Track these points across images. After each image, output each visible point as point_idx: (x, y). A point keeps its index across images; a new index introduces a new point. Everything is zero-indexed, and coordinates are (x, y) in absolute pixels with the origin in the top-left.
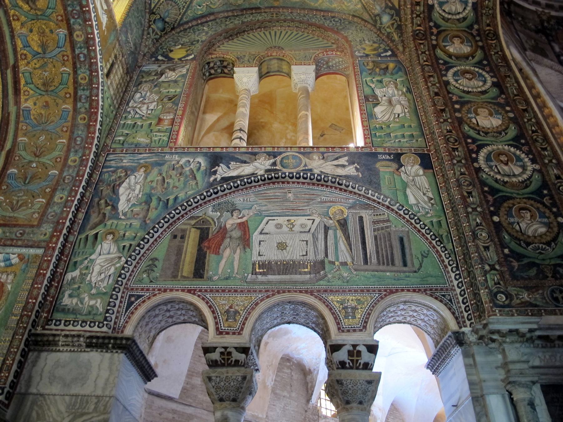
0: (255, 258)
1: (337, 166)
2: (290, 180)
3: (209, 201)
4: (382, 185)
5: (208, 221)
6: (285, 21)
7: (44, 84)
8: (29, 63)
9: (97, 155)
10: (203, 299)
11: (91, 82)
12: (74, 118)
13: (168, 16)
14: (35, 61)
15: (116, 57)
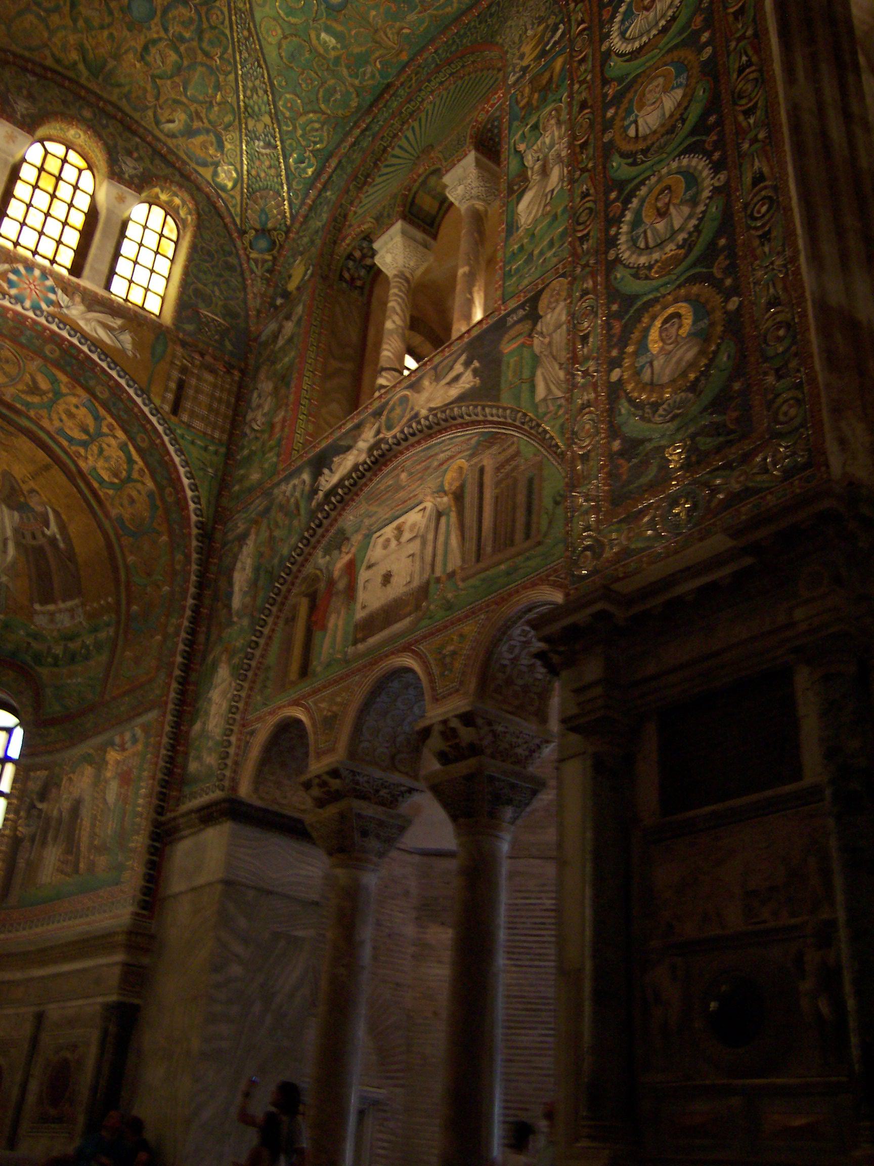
0: (360, 614)
1: (449, 384)
2: (400, 448)
3: (319, 542)
4: (503, 386)
5: (317, 576)
6: (429, 81)
7: (116, 475)
8: (86, 458)
9: (207, 535)
10: (306, 708)
11: (152, 442)
12: (162, 499)
13: (267, 219)
14: (89, 452)
15: (184, 370)
